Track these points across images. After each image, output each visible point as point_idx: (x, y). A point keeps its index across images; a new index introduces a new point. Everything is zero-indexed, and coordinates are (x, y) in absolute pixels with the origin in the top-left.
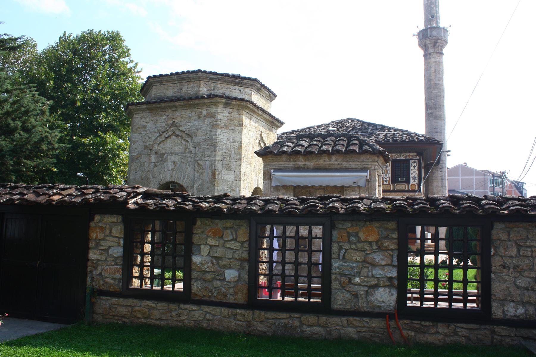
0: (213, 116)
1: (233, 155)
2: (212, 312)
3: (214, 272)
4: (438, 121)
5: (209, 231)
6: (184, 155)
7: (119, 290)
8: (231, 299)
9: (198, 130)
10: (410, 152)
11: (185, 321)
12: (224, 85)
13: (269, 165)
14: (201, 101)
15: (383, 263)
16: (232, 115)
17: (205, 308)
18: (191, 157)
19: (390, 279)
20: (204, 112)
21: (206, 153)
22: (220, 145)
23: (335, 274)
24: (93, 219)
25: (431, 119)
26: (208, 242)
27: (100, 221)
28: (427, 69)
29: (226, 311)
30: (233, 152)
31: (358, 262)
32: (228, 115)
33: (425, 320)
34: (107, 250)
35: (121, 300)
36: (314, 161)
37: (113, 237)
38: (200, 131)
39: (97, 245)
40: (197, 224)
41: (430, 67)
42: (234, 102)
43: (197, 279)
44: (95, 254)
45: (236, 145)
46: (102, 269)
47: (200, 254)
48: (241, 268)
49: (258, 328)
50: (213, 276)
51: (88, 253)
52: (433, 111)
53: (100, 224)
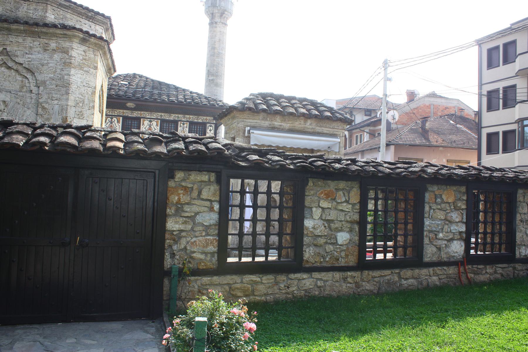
0: (65, 51)
1: (86, 101)
2: (323, 278)
3: (325, 236)
4: (218, 88)
5: (322, 193)
6: (21, 94)
7: (212, 266)
8: (342, 263)
9: (43, 66)
10: (207, 116)
11: (295, 292)
12: (75, 16)
13: (243, 121)
14: (52, 30)
15: (457, 220)
16: (88, 54)
17: (316, 275)
18: (31, 98)
19: (460, 233)
20: (53, 45)
21: (54, 95)
22: (73, 87)
23: (426, 231)
24: (173, 177)
25: (212, 85)
26: (320, 205)
27: (184, 180)
28: (212, 37)
29: (338, 275)
30: (86, 98)
31: (442, 220)
32: (83, 53)
33: (480, 264)
34: (192, 218)
35: (215, 278)
36: (291, 122)
37: (203, 200)
38: (45, 67)
39: (179, 210)
40: (309, 185)
41: (215, 36)
42: (92, 40)
43: (309, 246)
44: (176, 223)
45: (90, 90)
46: (188, 243)
47: (312, 217)
48: (351, 231)
49: (367, 288)
50: (325, 241)
51: (164, 222)
52: (214, 78)
53: (183, 184)
